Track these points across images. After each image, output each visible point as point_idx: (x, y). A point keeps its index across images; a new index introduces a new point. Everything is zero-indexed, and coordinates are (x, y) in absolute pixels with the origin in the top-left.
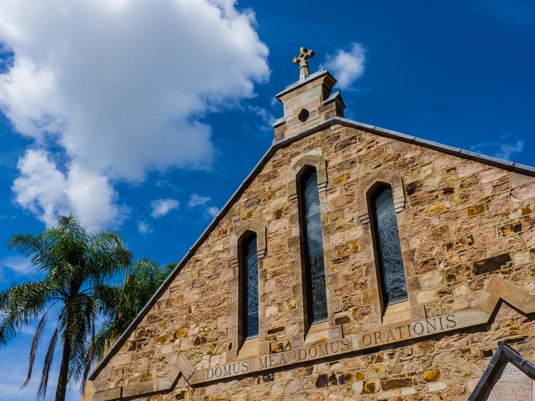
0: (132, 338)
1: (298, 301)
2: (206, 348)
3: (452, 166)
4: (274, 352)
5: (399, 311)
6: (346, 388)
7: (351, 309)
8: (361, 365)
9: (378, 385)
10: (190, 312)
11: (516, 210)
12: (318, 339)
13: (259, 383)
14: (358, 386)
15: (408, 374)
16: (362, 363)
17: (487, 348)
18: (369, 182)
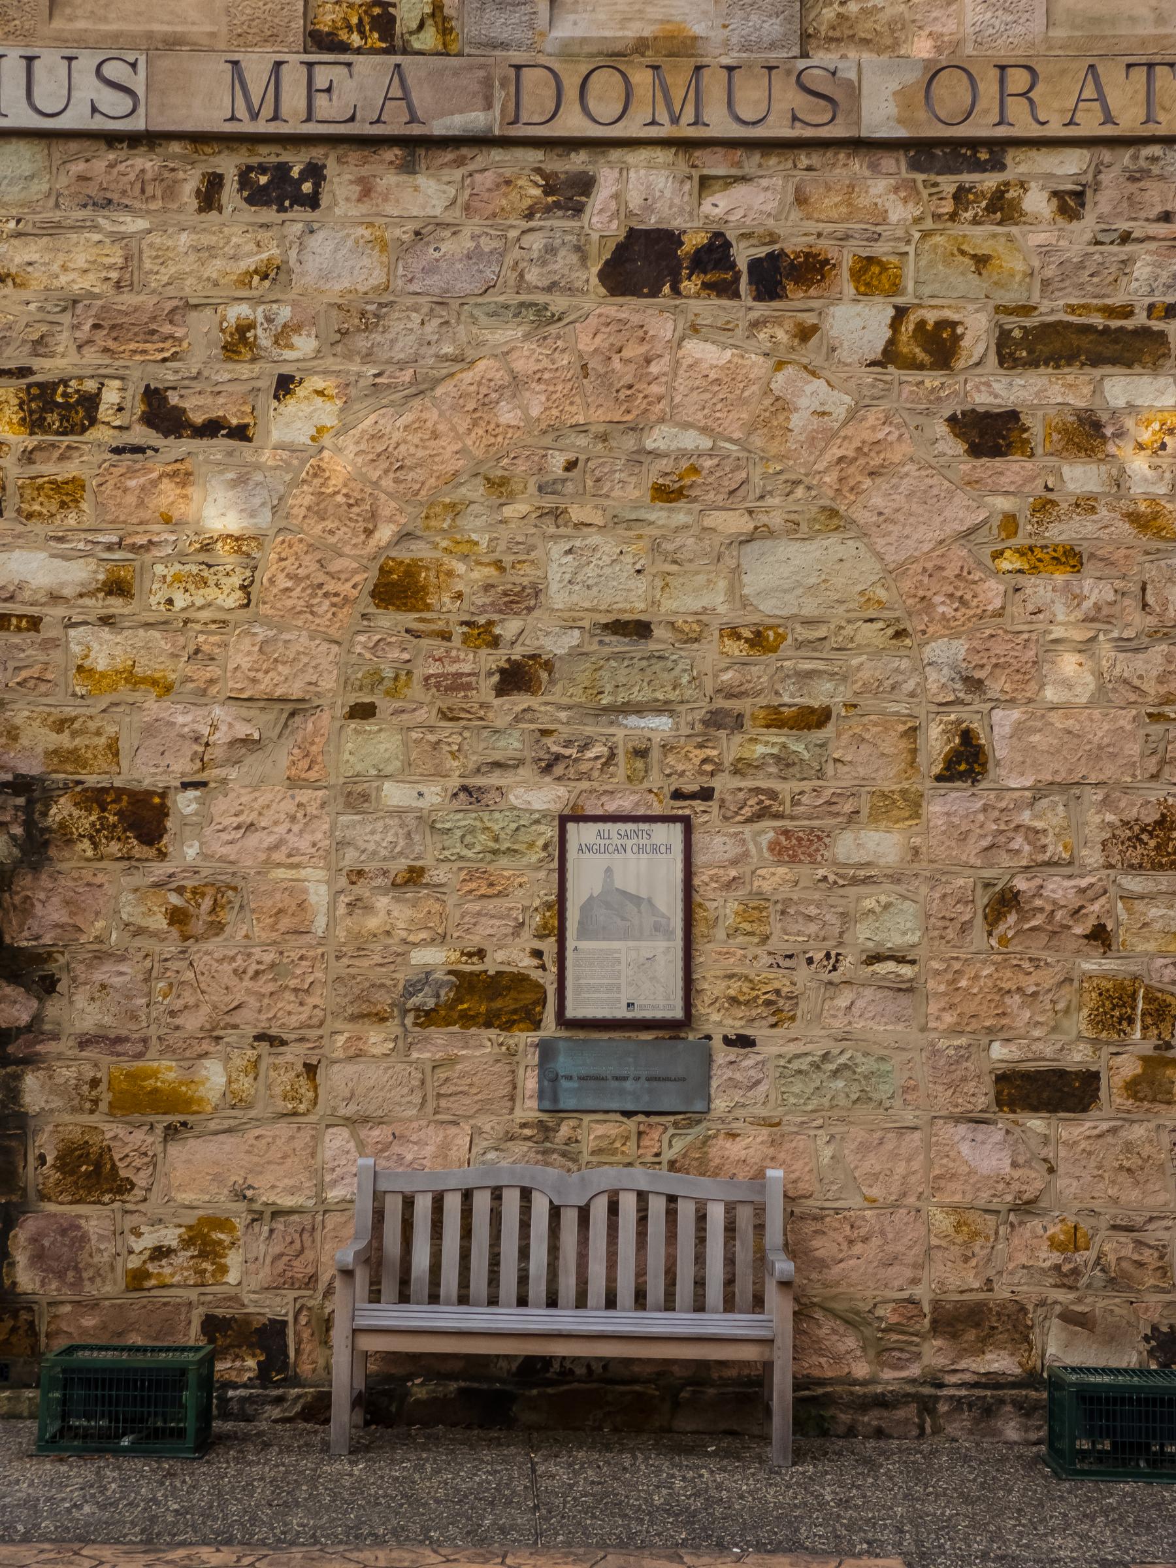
4: (323, 42)
6: (789, 325)
8: (893, 217)
9: (977, 332)
13: (209, 197)
14: (857, 324)
15: (1151, 308)
16: (899, 212)
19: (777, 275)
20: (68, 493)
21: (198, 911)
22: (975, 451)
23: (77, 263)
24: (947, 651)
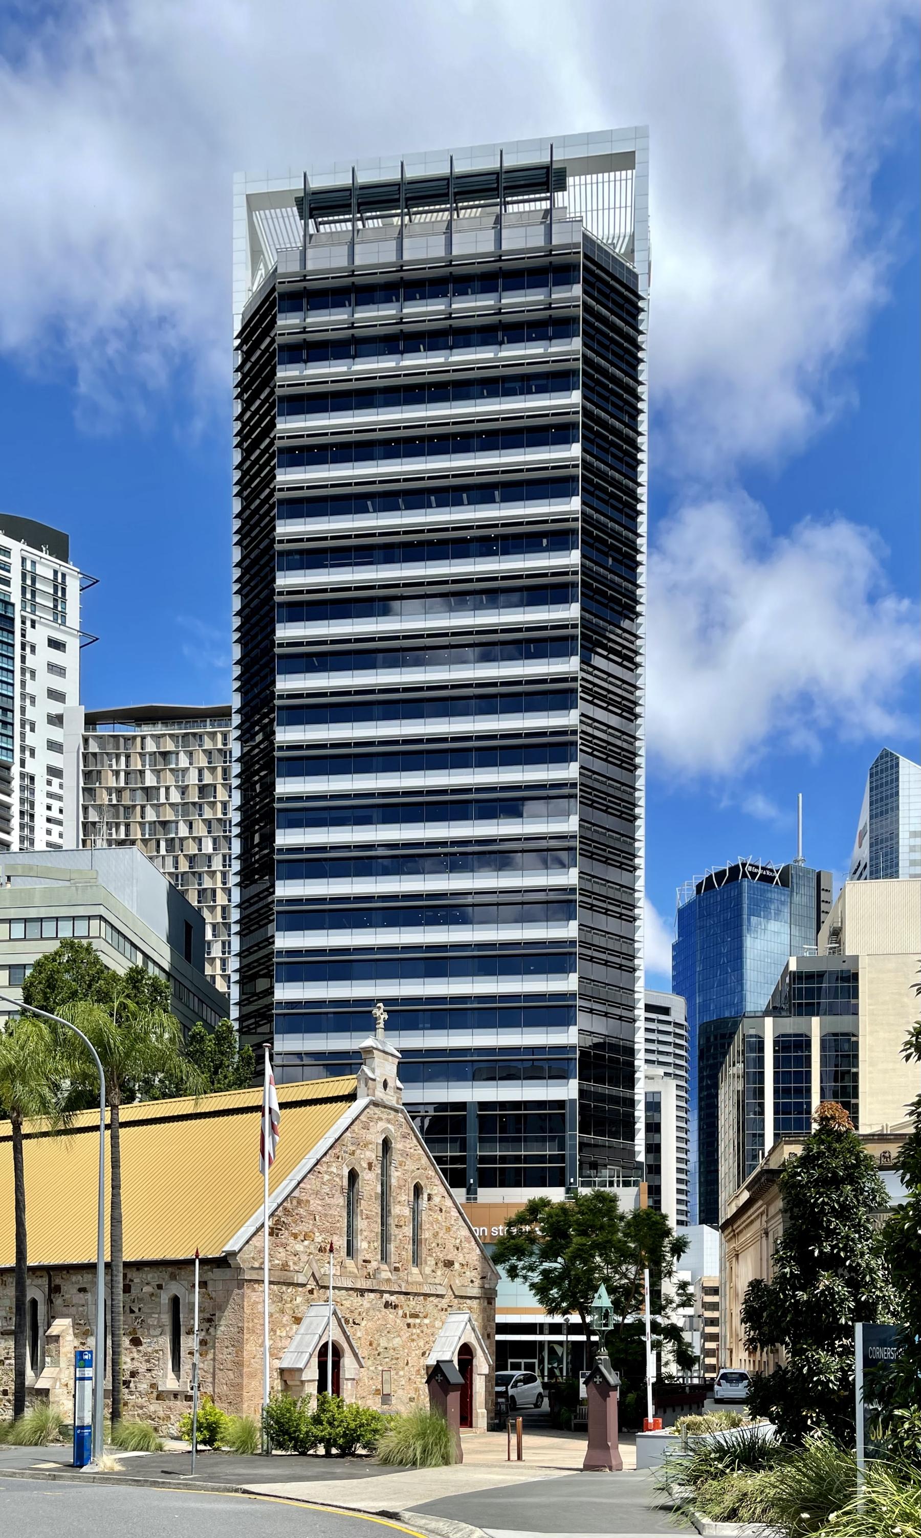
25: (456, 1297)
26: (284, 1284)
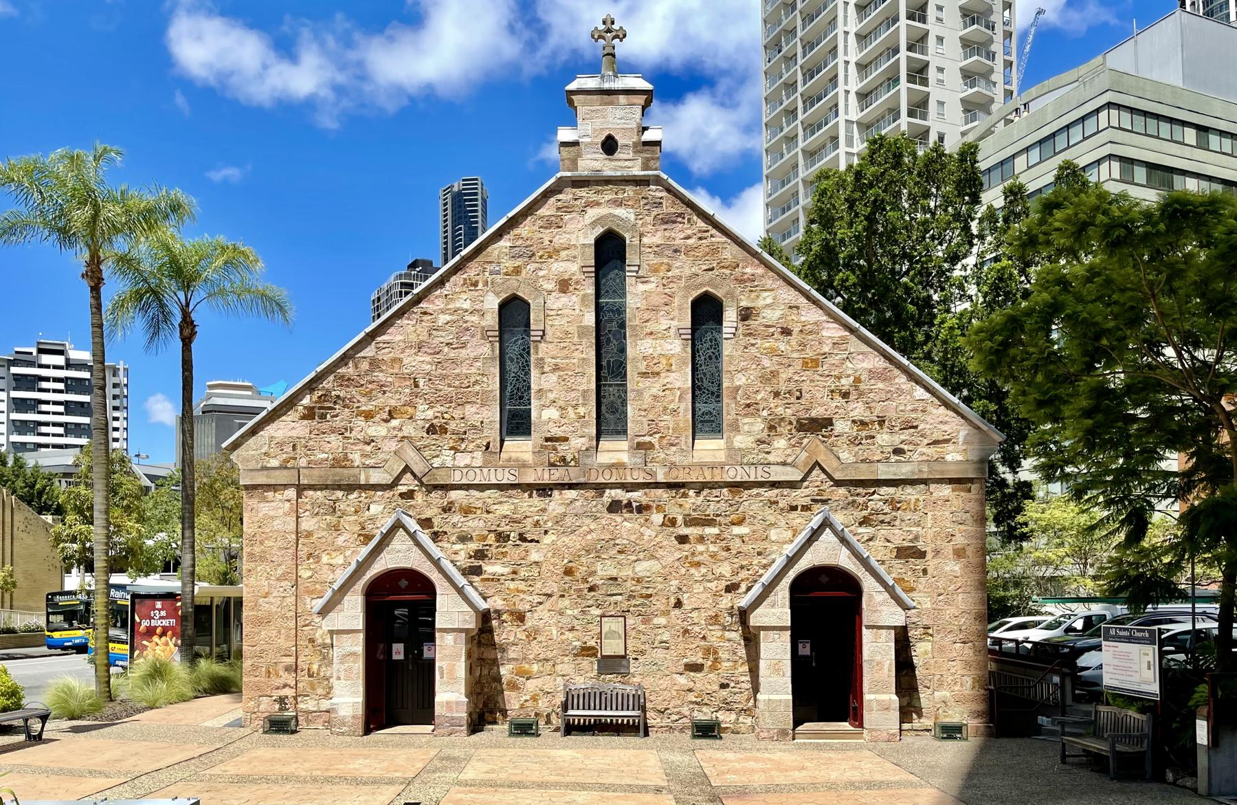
0: (306, 401)
1: (589, 409)
2: (448, 441)
3: (794, 303)
4: (552, 465)
5: (709, 448)
7: (657, 436)
10: (417, 386)
11: (849, 376)
12: (614, 461)
13: (530, 496)
17: (794, 504)
18: (697, 287)
19: (641, 509)
20: (504, 554)
21: (532, 635)
22: (680, 543)
23: (505, 509)
24: (675, 583)
25: (838, 483)
26: (339, 487)
